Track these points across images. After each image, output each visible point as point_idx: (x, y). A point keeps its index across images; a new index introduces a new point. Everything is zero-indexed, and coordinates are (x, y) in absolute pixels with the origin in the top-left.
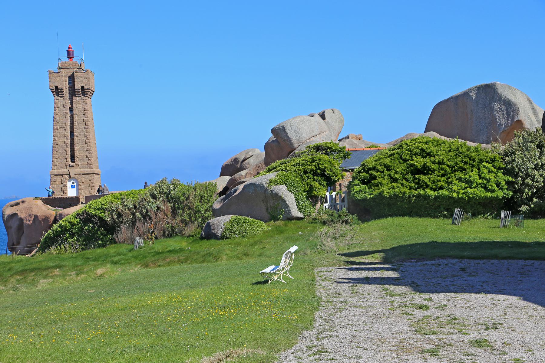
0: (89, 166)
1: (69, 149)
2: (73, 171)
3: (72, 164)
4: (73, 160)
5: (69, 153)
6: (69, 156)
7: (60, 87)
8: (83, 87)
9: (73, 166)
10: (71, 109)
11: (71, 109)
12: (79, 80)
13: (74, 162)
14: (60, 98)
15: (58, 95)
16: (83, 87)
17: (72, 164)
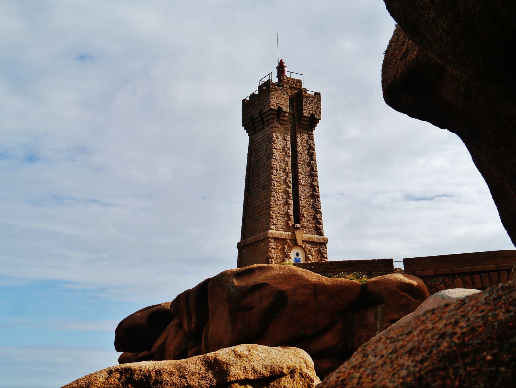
0: (319, 231)
1: (291, 201)
2: (301, 236)
3: (298, 225)
4: (298, 218)
5: (292, 208)
6: (291, 212)
7: (285, 108)
8: (313, 115)
9: (298, 228)
10: (294, 144)
11: (294, 144)
12: (308, 105)
13: (299, 223)
14: (279, 126)
15: (278, 121)
16: (313, 115)
17: (298, 225)
